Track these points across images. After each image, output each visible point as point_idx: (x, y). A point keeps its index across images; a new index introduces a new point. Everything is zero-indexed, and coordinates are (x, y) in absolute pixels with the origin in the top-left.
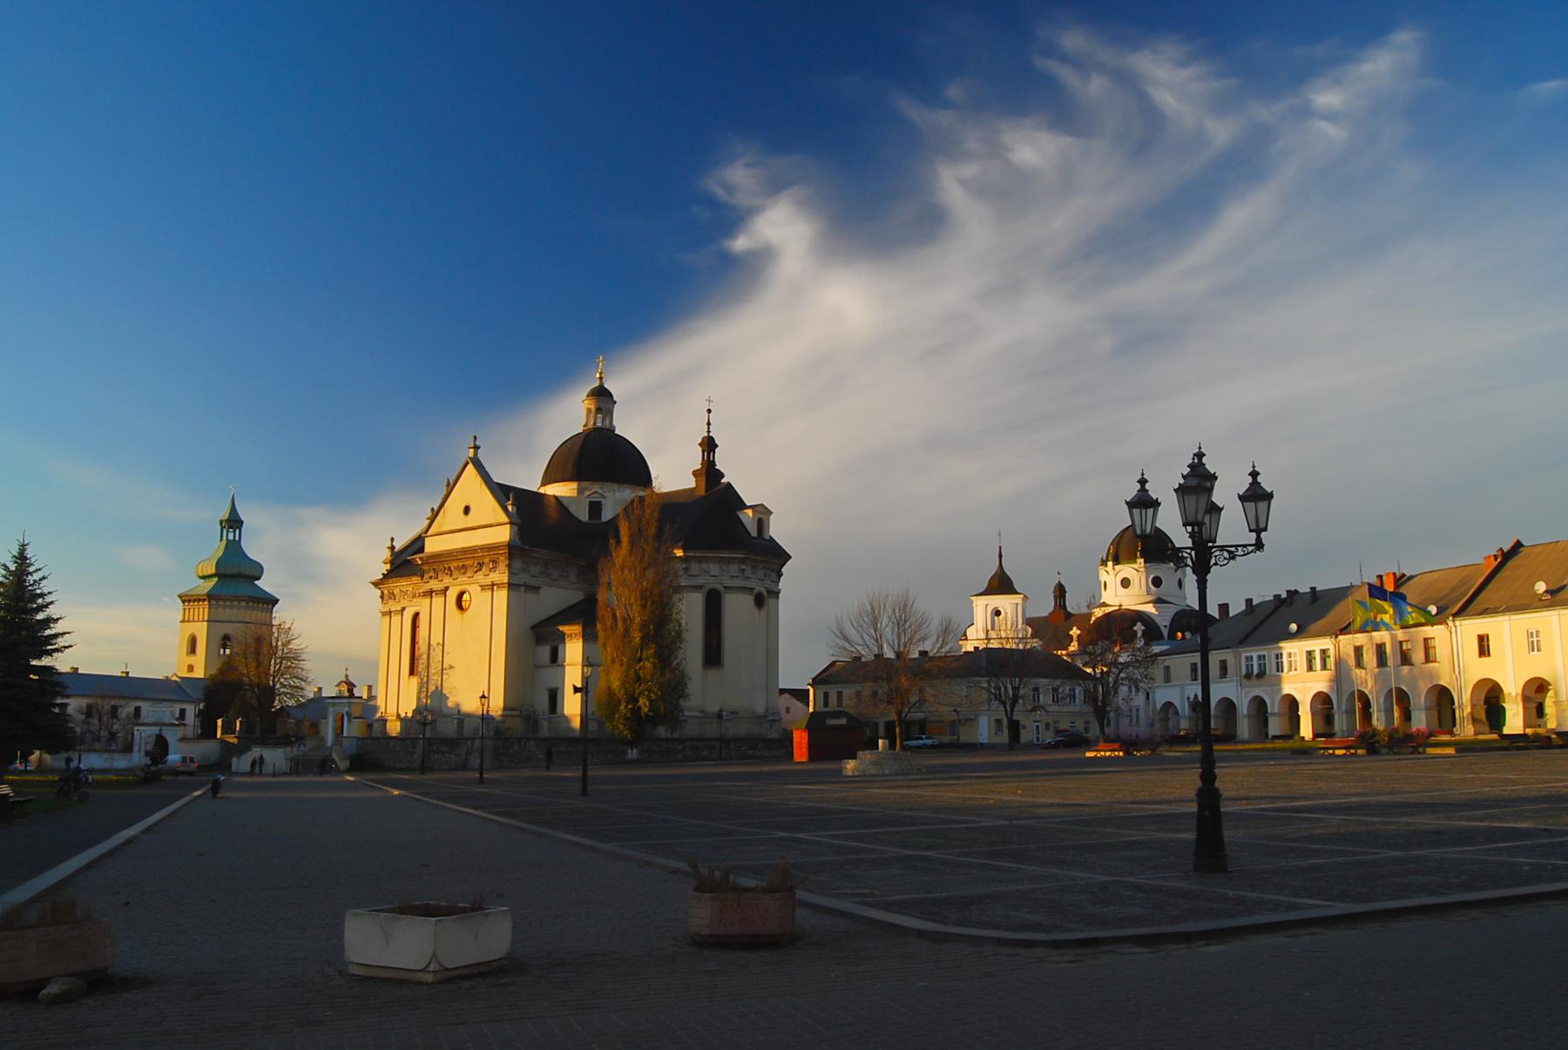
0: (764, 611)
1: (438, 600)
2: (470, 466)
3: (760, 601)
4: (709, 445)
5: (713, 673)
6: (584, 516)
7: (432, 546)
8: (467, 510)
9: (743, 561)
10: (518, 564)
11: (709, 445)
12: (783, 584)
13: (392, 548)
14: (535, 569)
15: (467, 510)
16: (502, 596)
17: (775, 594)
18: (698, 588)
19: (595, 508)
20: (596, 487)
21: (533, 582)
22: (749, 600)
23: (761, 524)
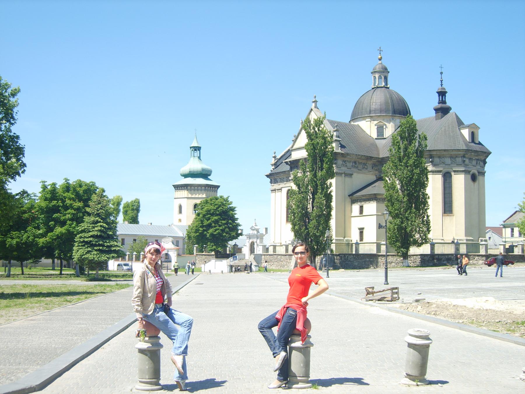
0: (476, 183)
3: (474, 178)
4: (442, 94)
5: (447, 219)
6: (374, 135)
11: (442, 94)
12: (487, 168)
14: (349, 165)
17: (483, 174)
18: (440, 171)
19: (380, 130)
22: (469, 177)
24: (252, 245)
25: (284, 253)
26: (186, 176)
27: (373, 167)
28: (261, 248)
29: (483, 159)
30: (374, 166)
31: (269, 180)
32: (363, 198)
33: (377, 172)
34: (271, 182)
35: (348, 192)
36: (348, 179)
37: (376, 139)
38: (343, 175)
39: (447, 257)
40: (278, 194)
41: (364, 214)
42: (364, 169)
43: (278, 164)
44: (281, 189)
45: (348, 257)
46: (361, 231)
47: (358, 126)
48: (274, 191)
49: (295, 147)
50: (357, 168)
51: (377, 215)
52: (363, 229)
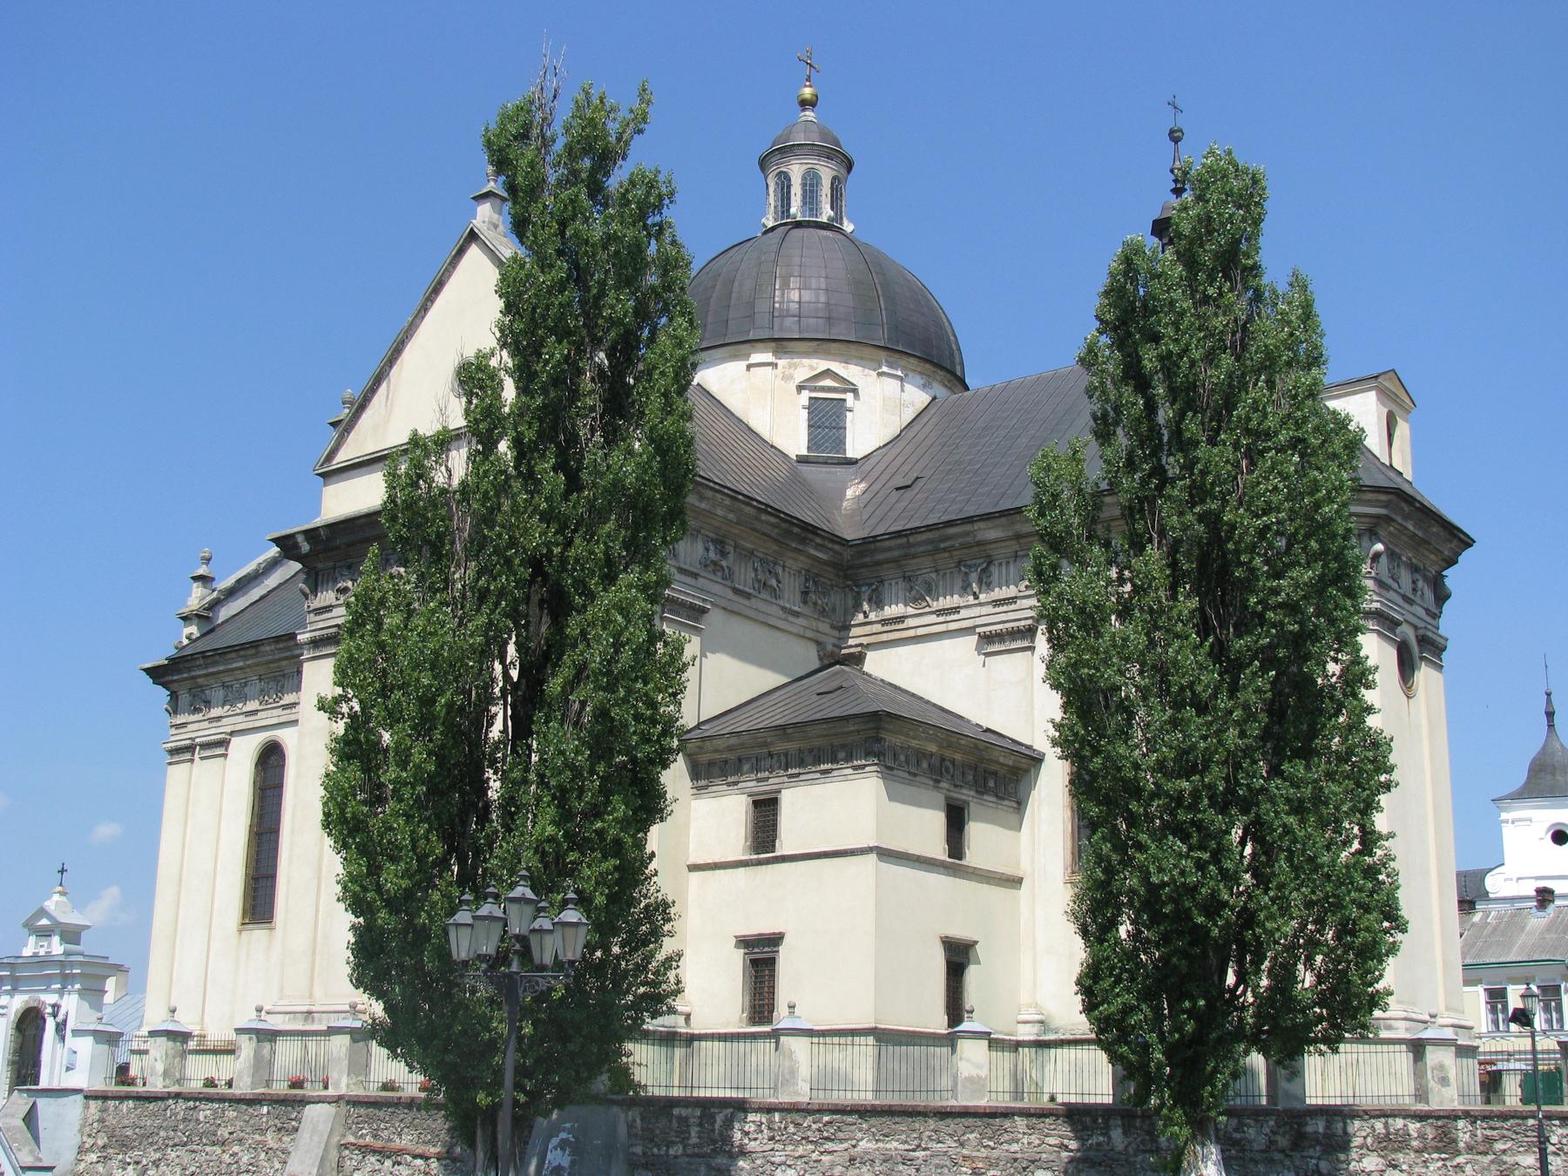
6: (793, 439)
19: (827, 419)
27: (805, 593)
29: (1433, 571)
30: (812, 585)
31: (162, 694)
32: (780, 746)
33: (824, 627)
34: (174, 709)
37: (802, 460)
39: (1379, 1125)
40: (203, 770)
41: (785, 846)
42: (764, 595)
44: (224, 743)
46: (761, 957)
50: (728, 576)
52: (775, 940)
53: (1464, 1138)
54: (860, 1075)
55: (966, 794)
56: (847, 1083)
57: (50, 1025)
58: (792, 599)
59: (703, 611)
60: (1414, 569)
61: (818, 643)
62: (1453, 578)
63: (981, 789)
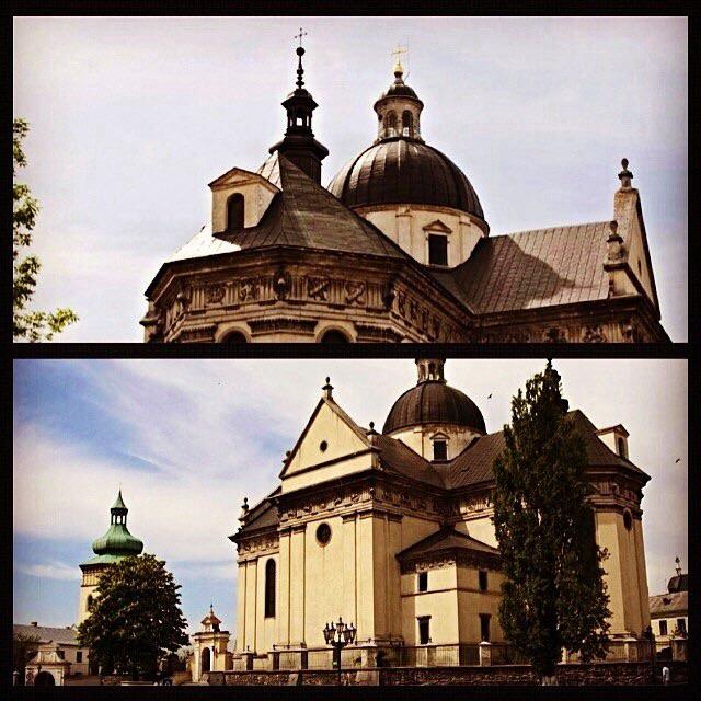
1: (297, 537)
2: (324, 406)
6: (430, 457)
7: (290, 486)
8: (324, 446)
9: (611, 478)
10: (380, 492)
13: (246, 507)
14: (396, 498)
15: (324, 446)
16: (366, 525)
17: (639, 514)
19: (440, 449)
20: (440, 430)
21: (396, 510)
22: (622, 517)
23: (621, 444)
24: (206, 653)
25: (271, 669)
26: (99, 551)
28: (222, 658)
31: (235, 545)
34: (238, 550)
35: (393, 550)
36: (394, 525)
38: (386, 517)
40: (251, 567)
43: (251, 519)
44: (256, 560)
45: (413, 675)
47: (399, 440)
48: (243, 563)
49: (288, 472)
51: (459, 589)
53: (639, 671)
54: (453, 659)
55: (486, 570)
56: (451, 660)
57: (212, 653)
58: (430, 510)
59: (401, 517)
60: (629, 489)
61: (440, 523)
62: (644, 490)
63: (491, 569)
